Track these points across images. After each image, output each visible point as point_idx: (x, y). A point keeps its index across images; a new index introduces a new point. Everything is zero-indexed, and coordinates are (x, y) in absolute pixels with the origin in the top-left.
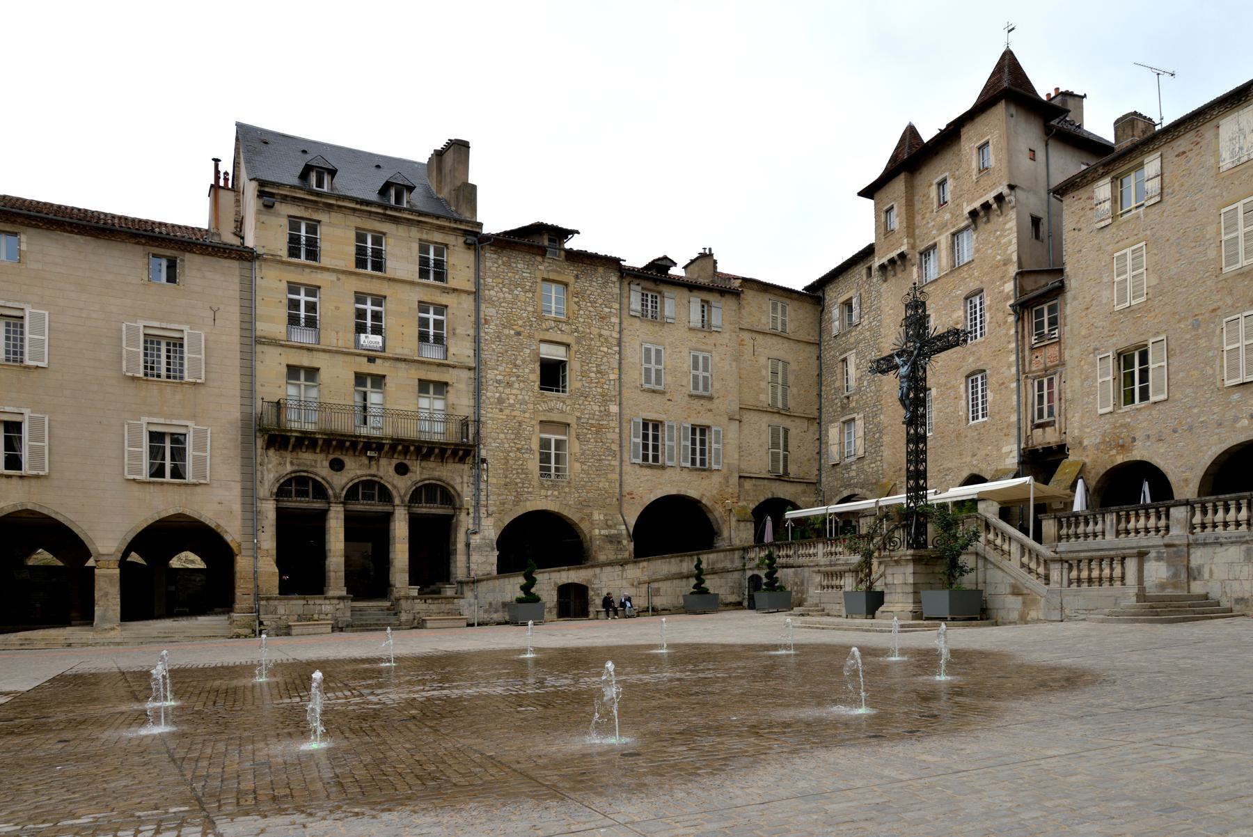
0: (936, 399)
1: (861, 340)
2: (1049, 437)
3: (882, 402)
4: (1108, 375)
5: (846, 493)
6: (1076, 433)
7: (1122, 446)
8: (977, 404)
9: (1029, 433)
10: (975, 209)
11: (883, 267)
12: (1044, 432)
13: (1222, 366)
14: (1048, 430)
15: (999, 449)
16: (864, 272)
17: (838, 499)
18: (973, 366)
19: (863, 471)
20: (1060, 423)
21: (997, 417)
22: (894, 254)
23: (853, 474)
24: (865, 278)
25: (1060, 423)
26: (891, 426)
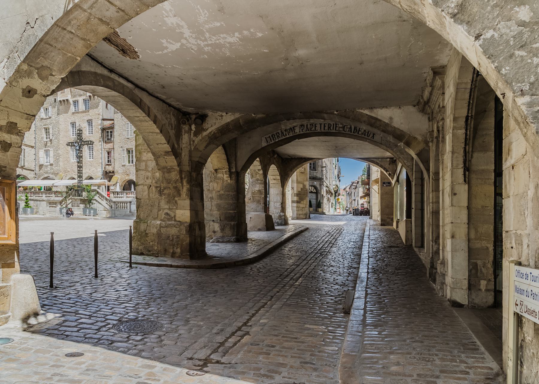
5: (46, 175)
11: (60, 101)
17: (43, 177)
19: (52, 169)
23: (49, 169)
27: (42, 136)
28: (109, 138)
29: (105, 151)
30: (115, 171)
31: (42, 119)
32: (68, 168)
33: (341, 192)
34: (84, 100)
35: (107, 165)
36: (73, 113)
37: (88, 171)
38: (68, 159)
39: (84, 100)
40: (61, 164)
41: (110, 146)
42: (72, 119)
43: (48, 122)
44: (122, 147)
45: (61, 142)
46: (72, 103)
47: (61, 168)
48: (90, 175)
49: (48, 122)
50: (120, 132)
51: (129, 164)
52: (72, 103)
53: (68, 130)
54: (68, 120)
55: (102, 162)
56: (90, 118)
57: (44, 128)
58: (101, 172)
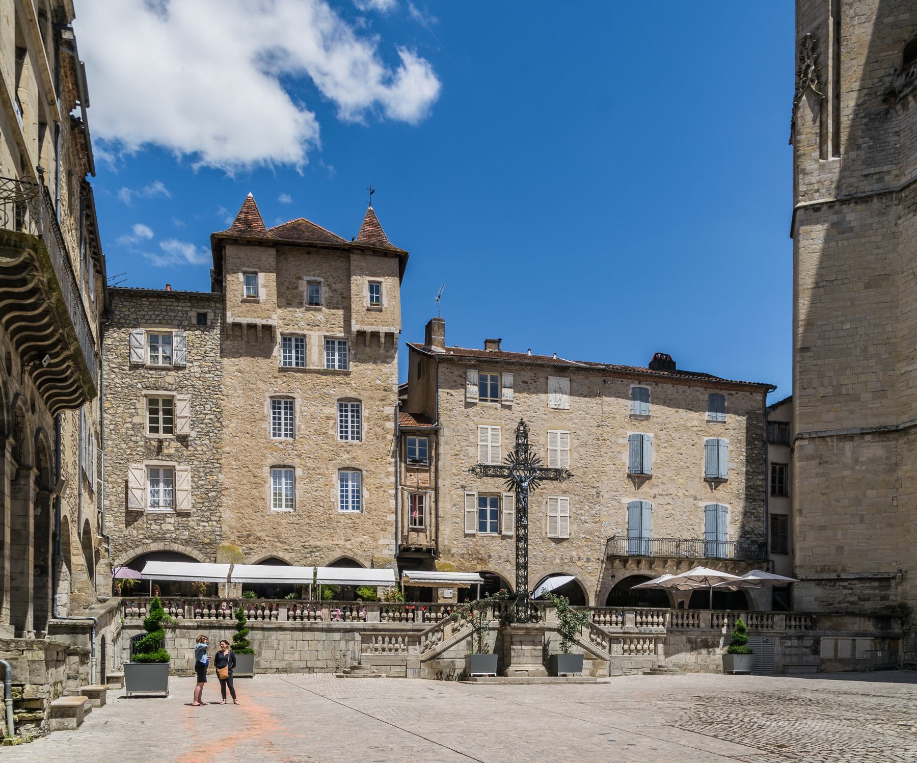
0: (302, 479)
1: (186, 386)
2: (422, 540)
3: (222, 461)
4: (473, 507)
6: (447, 542)
7: (481, 559)
8: (347, 497)
9: (406, 533)
10: (365, 332)
12: (418, 536)
13: (546, 524)
14: (422, 535)
15: (375, 540)
16: (193, 314)
18: (348, 462)
20: (431, 532)
21: (374, 513)
22: (259, 322)
24: (194, 321)
25: (431, 532)
26: (236, 489)
27: (136, 420)
28: (417, 456)
29: (406, 493)
30: (440, 547)
31: (135, 367)
32: (257, 528)
33: (428, 653)
34: (325, 337)
35: (414, 530)
36: (281, 370)
37: (341, 542)
38: (259, 503)
39: (325, 337)
40: (227, 515)
41: (422, 478)
42: (280, 387)
43: (170, 379)
44: (463, 487)
45: (227, 449)
46: (279, 338)
47: (225, 528)
48: (350, 554)
49: (170, 379)
50: (458, 447)
51: (483, 534)
52: (279, 338)
53: (258, 417)
54: (262, 386)
55: (397, 521)
56: (353, 394)
57: (145, 396)
58: (393, 547)
